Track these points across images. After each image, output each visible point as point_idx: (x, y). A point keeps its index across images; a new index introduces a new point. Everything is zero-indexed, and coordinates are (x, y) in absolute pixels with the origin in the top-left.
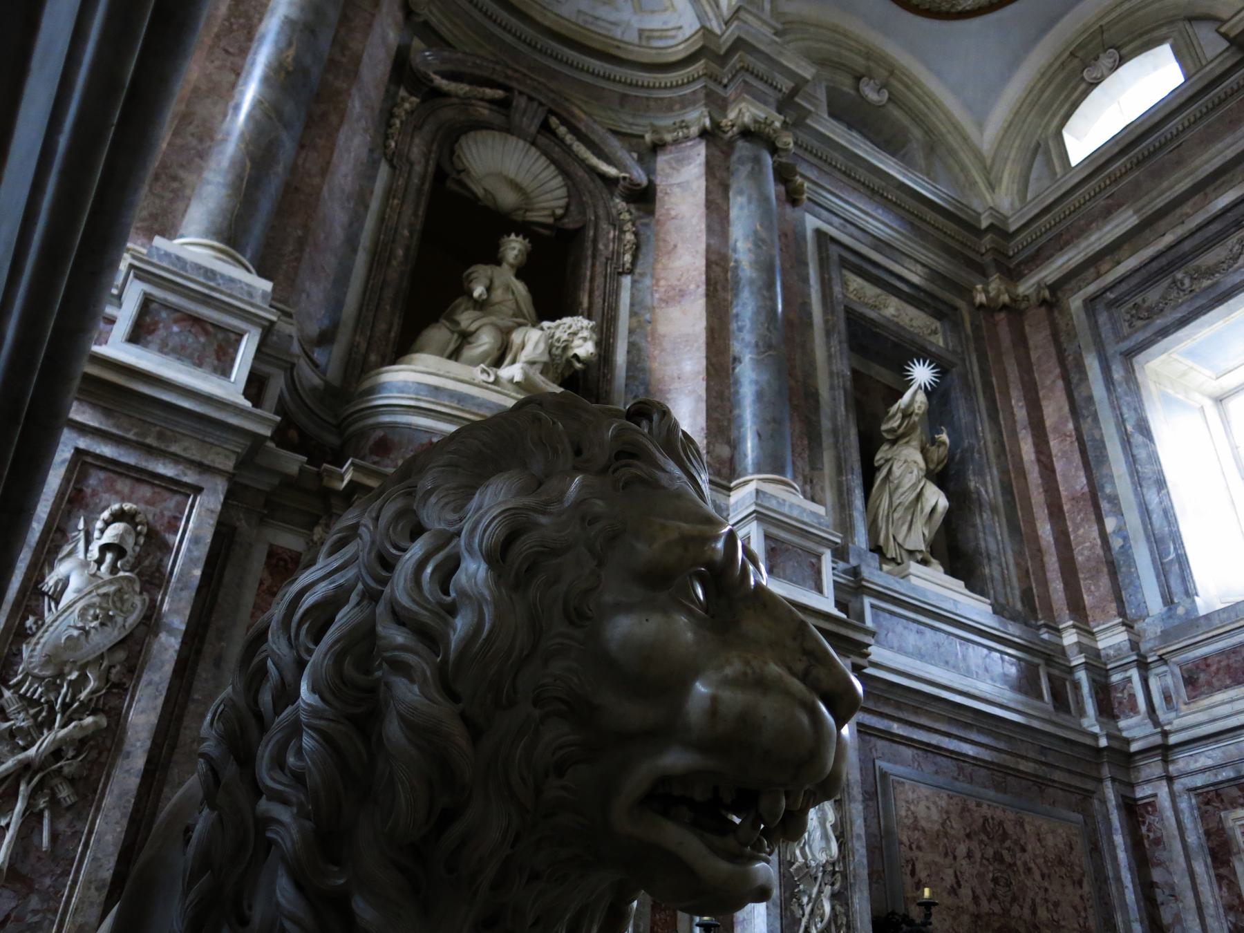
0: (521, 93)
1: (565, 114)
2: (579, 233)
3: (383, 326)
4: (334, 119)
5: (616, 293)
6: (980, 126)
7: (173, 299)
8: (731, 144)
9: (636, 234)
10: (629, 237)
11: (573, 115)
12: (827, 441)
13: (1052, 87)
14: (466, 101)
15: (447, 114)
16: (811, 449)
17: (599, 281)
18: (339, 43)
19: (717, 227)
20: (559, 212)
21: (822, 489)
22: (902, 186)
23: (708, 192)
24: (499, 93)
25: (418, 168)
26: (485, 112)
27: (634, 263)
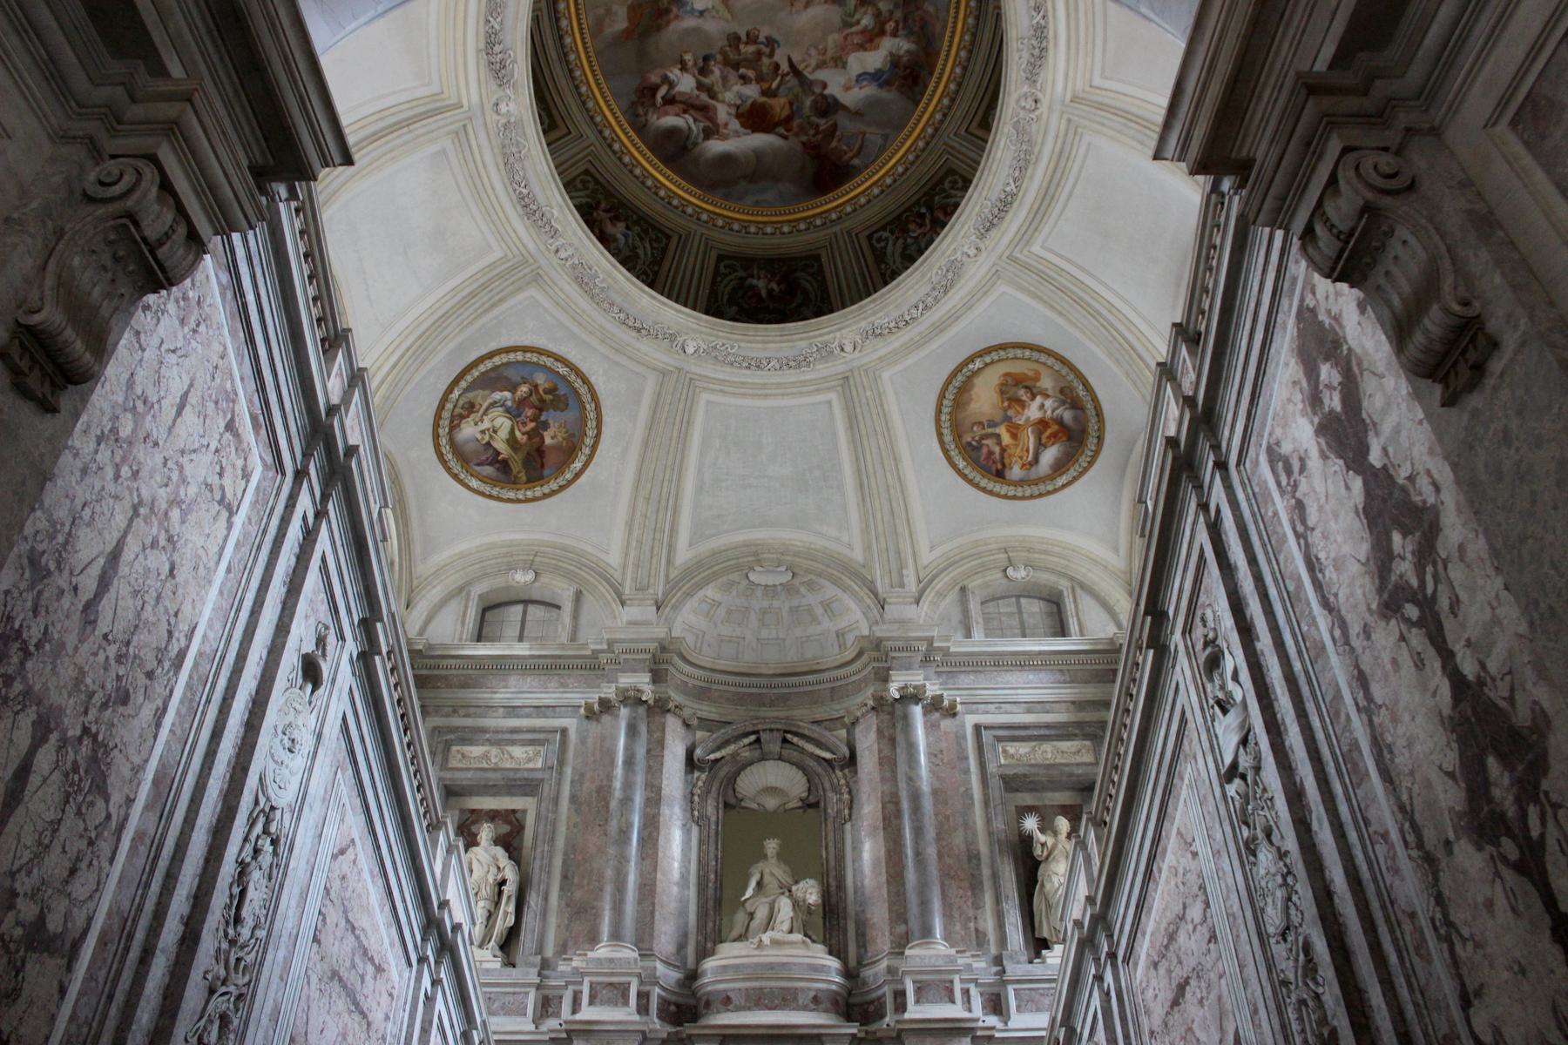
3: (710, 925)
7: (600, 979)
8: (892, 705)
9: (850, 792)
10: (846, 796)
12: (987, 884)
14: (734, 755)
15: (724, 771)
16: (974, 895)
17: (831, 835)
20: (805, 795)
22: (1040, 653)
23: (880, 751)
24: (753, 738)
25: (713, 819)
26: (746, 754)
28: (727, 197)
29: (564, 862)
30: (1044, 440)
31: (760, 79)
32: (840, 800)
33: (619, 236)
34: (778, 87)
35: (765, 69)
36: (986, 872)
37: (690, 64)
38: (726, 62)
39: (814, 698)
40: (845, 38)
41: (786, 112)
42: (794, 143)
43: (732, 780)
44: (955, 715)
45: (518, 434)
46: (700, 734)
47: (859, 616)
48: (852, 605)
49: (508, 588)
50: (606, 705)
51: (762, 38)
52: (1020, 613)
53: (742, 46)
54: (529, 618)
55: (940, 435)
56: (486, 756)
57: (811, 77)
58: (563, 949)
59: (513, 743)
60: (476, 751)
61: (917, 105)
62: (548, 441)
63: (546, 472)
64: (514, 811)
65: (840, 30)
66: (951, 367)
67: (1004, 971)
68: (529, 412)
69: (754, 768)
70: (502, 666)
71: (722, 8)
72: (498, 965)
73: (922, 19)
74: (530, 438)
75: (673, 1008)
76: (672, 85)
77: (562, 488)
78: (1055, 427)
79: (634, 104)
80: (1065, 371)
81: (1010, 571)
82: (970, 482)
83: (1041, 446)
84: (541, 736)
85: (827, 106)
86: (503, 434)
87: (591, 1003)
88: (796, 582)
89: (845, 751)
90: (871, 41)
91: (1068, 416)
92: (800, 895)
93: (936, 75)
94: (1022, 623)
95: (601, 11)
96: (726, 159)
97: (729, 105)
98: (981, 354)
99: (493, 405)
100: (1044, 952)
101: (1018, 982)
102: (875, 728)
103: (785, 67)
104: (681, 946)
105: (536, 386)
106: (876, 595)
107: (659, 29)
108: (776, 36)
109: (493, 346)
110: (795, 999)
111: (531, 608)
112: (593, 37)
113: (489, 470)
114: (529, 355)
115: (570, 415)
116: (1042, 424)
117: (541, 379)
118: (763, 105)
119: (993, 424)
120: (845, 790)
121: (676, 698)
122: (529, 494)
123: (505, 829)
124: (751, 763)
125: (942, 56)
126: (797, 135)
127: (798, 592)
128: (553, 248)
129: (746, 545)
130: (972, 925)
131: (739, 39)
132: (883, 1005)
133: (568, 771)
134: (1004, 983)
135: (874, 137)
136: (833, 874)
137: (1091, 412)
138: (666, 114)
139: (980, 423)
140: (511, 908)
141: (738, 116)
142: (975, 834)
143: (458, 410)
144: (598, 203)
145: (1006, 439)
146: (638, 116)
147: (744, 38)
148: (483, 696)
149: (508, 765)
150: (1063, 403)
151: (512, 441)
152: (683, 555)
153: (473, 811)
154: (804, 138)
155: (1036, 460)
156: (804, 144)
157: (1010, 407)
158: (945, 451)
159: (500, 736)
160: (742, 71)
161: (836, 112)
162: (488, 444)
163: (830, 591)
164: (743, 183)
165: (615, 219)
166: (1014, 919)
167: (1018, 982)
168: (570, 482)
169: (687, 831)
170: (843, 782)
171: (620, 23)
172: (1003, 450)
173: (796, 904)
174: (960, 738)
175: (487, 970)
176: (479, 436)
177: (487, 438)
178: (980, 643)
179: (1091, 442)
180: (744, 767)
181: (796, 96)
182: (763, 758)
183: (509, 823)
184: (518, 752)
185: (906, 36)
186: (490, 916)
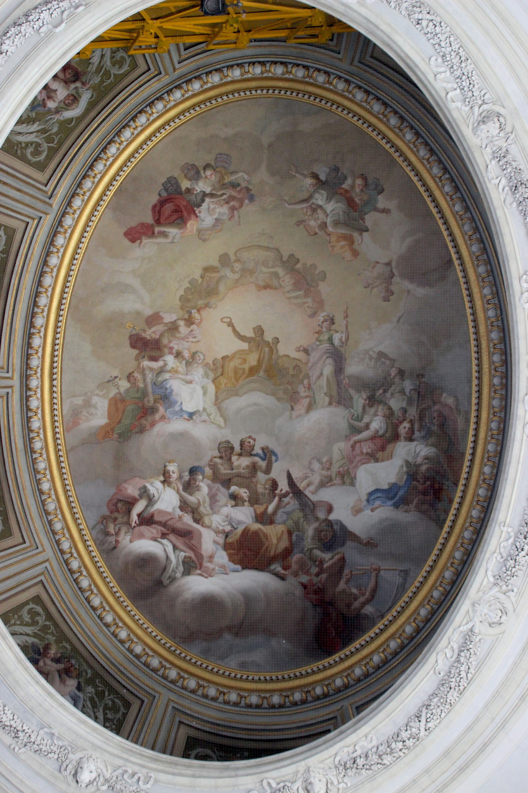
28: (206, 653)
31: (254, 500)
34: (275, 512)
35: (260, 489)
37: (175, 476)
38: (216, 477)
40: (353, 447)
41: (284, 544)
42: (292, 585)
51: (257, 450)
53: (234, 458)
57: (314, 498)
61: (442, 528)
65: (347, 438)
71: (213, 410)
73: (440, 414)
76: (151, 501)
79: (104, 518)
85: (334, 536)
90: (383, 448)
93: (462, 482)
95: (79, 401)
96: (208, 603)
97: (217, 532)
103: (283, 486)
107: (142, 430)
108: (273, 445)
112: (67, 430)
118: (256, 533)
125: (468, 457)
126: (296, 575)
131: (232, 448)
135: (390, 577)
138: (142, 536)
141: (227, 547)
144: (47, 647)
146: (107, 534)
147: (237, 448)
154: (304, 579)
156: (305, 586)
160: (233, 488)
161: (343, 545)
164: (227, 637)
165: (67, 672)
171: (99, 418)
181: (297, 523)
185: (424, 438)
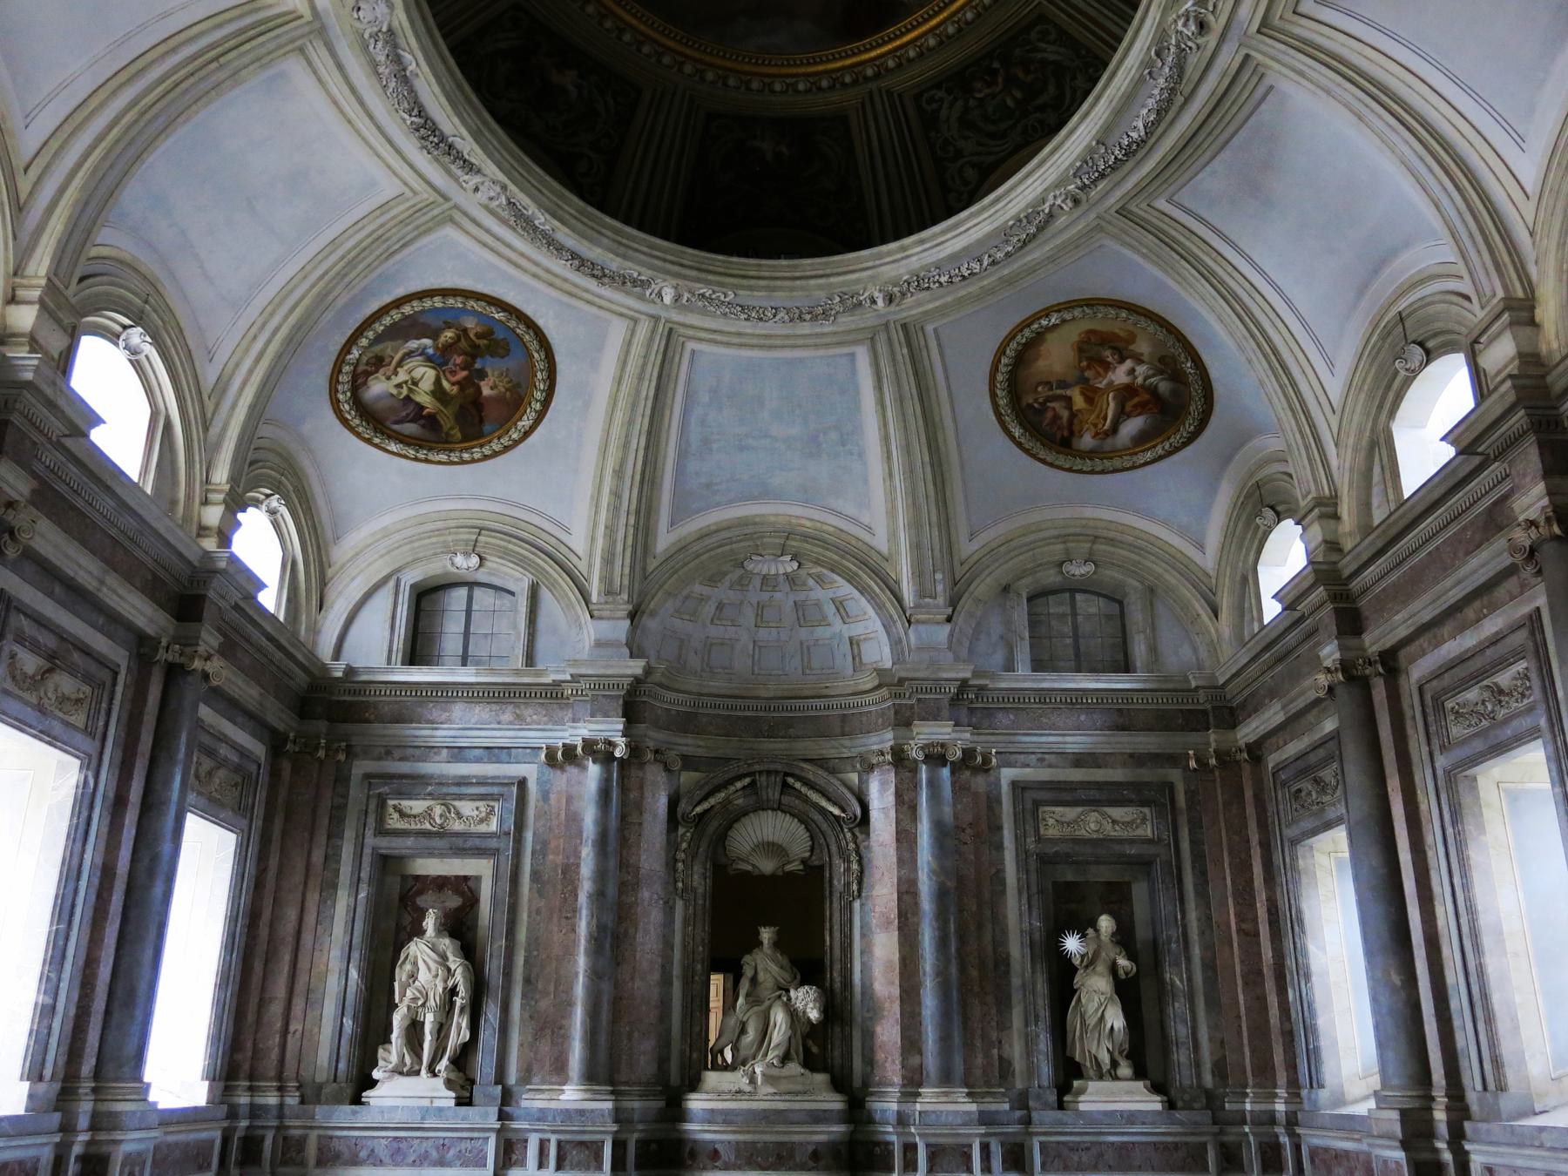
0: (760, 772)
1: (797, 772)
2: (821, 868)
4: (631, 931)
5: (851, 920)
6: (1201, 547)
10: (855, 866)
11: (802, 769)
12: (1016, 998)
13: (1240, 525)
15: (713, 826)
17: (836, 915)
18: (623, 865)
19: (907, 855)
21: (1011, 1046)
24: (747, 781)
25: (700, 891)
27: (860, 891)
29: (526, 962)
30: (1128, 408)
32: (848, 869)
33: (571, 88)
36: (1016, 981)
39: (820, 728)
43: (721, 838)
44: (987, 771)
45: (445, 384)
46: (688, 778)
47: (879, 626)
48: (871, 611)
49: (447, 574)
50: (570, 756)
52: (1074, 614)
54: (475, 607)
55: (993, 395)
56: (428, 813)
58: (526, 1077)
59: (460, 797)
60: (417, 806)
62: (486, 391)
63: (487, 428)
64: (466, 878)
66: (1018, 320)
67: (1028, 1121)
68: (459, 360)
69: (745, 820)
70: (444, 693)
72: (452, 1103)
74: (462, 389)
75: (654, 1146)
77: (506, 449)
78: (1146, 397)
80: (1171, 341)
81: (1066, 567)
82: (1027, 451)
83: (1122, 415)
84: (495, 790)
86: (427, 384)
87: (559, 1167)
88: (803, 572)
89: (859, 812)
91: (1164, 387)
92: (800, 1005)
94: (1075, 627)
98: (1058, 308)
99: (409, 354)
100: (1076, 1083)
101: (1045, 1134)
102: (893, 789)
104: (663, 1061)
105: (465, 331)
106: (900, 600)
109: (400, 292)
110: (792, 1156)
111: (477, 592)
113: (410, 428)
114: (451, 301)
115: (512, 363)
116: (1127, 392)
117: (470, 323)
119: (1063, 384)
120: (854, 857)
121: (653, 737)
122: (466, 456)
123: (454, 902)
124: (746, 814)
127: (804, 584)
128: (471, 185)
129: (743, 522)
130: (995, 1051)
132: (891, 1154)
133: (529, 836)
134: (1031, 1134)
136: (837, 966)
137: (1196, 390)
139: (1048, 384)
140: (465, 1023)
142: (1004, 932)
143: (361, 368)
145: (1079, 402)
148: (422, 733)
149: (457, 826)
150: (1161, 372)
151: (438, 392)
152: (664, 540)
153: (417, 878)
155: (1114, 430)
157: (1088, 367)
158: (998, 415)
159: (445, 790)
162: (408, 398)
163: (845, 589)
166: (1044, 1043)
167: (1045, 1134)
168: (516, 443)
169: (669, 909)
170: (852, 846)
172: (1073, 415)
173: (794, 1015)
174: (993, 801)
175: (440, 1109)
176: (394, 392)
177: (405, 391)
178: (1024, 678)
179: (1189, 426)
180: (737, 820)
182: (761, 807)
183: (458, 892)
184: (467, 808)
186: (442, 1031)
